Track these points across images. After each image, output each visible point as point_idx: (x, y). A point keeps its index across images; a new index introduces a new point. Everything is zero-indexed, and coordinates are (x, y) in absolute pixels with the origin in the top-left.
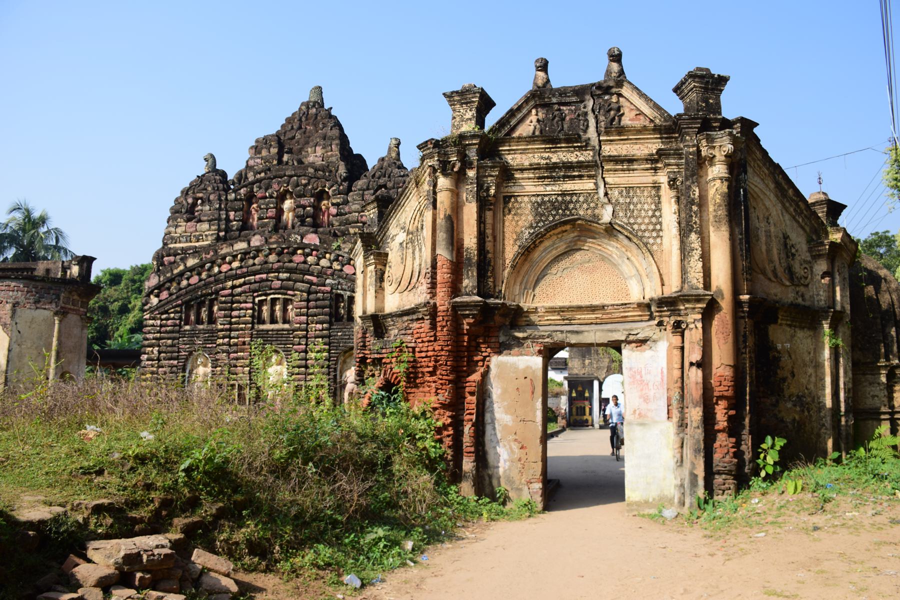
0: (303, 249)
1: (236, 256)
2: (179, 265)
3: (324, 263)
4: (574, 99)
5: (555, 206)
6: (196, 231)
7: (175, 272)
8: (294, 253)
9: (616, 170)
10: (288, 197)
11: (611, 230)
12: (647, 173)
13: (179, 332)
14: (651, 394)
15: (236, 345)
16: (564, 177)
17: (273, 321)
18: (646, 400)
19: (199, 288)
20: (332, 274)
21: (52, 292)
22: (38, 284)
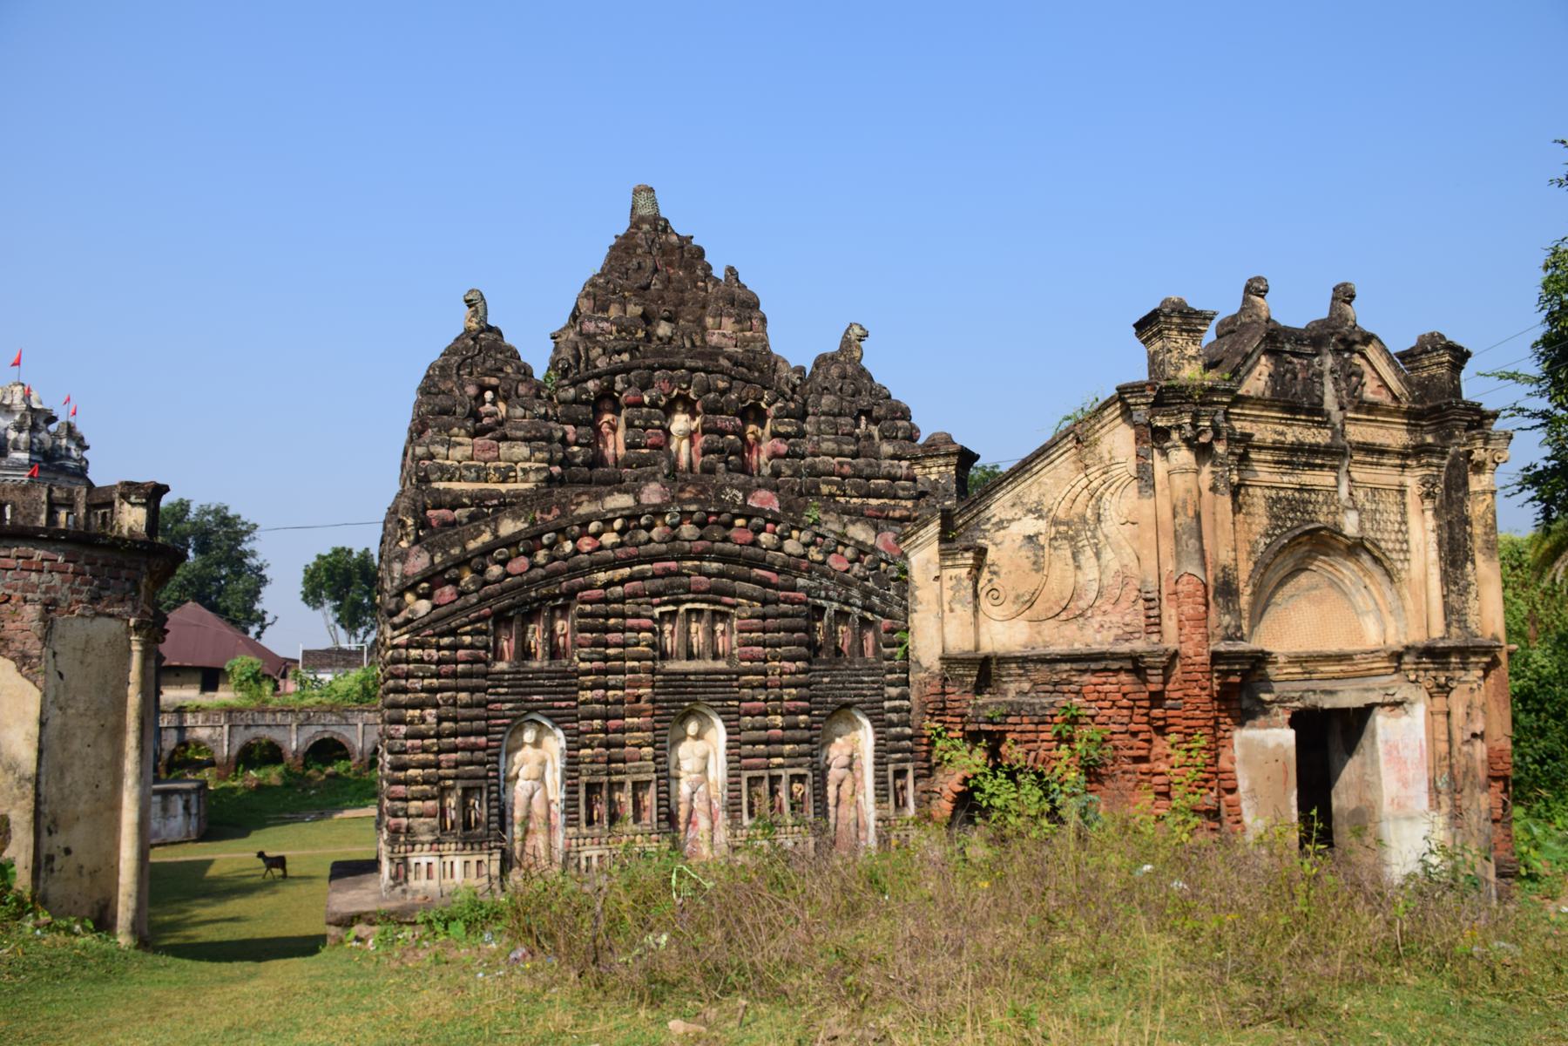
0: (748, 518)
1: (614, 519)
2: (481, 533)
3: (791, 546)
4: (1309, 350)
5: (1292, 506)
6: (498, 459)
7: (472, 545)
8: (729, 525)
9: (1364, 463)
10: (680, 408)
11: (1356, 548)
12: (1395, 471)
13: (485, 675)
14: (1410, 775)
15: (620, 701)
16: (1307, 464)
17: (690, 656)
18: (1405, 784)
19: (532, 582)
20: (809, 571)
21: (124, 573)
22: (96, 554)
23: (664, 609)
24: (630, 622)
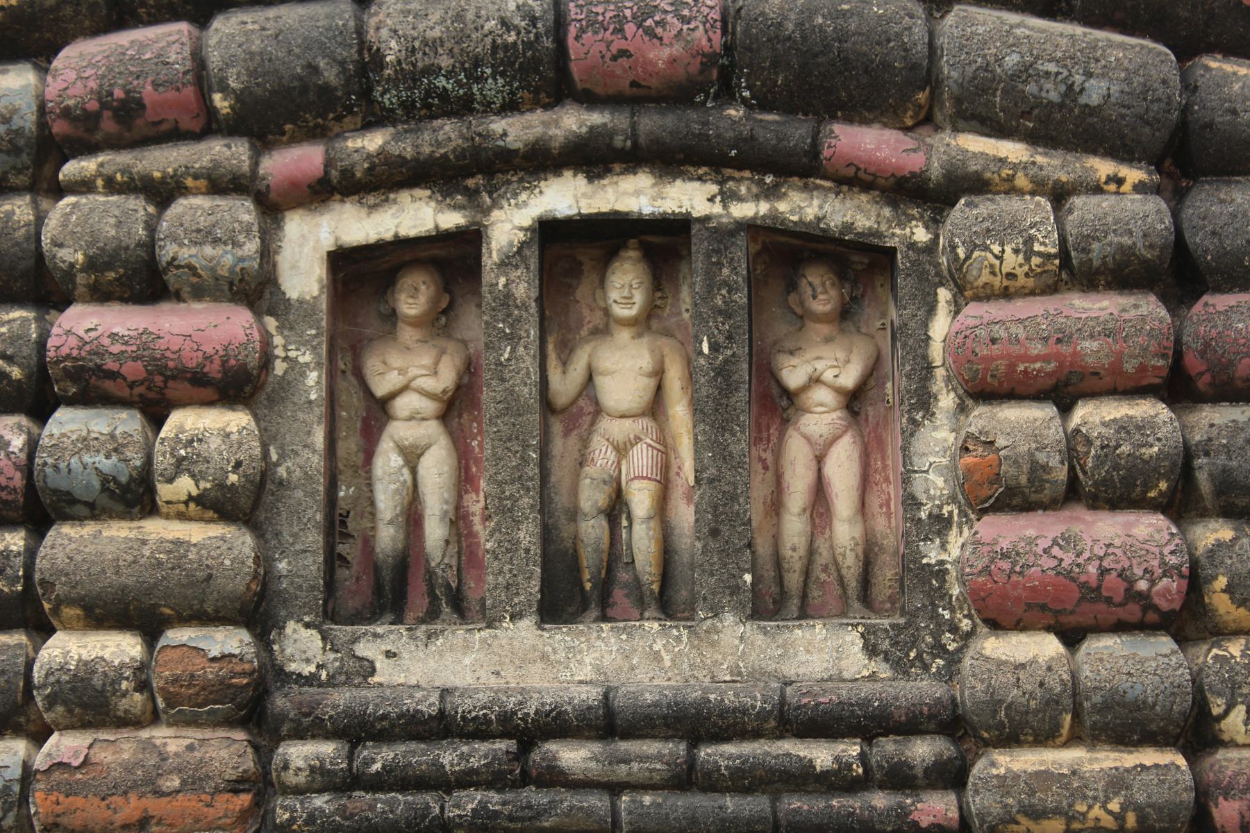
23: (359, 225)
24: (85, 325)
